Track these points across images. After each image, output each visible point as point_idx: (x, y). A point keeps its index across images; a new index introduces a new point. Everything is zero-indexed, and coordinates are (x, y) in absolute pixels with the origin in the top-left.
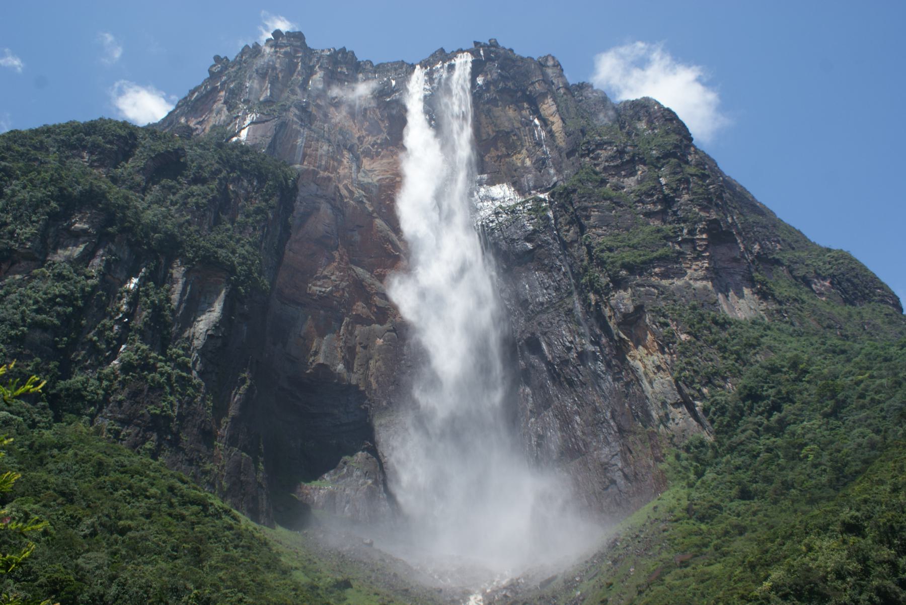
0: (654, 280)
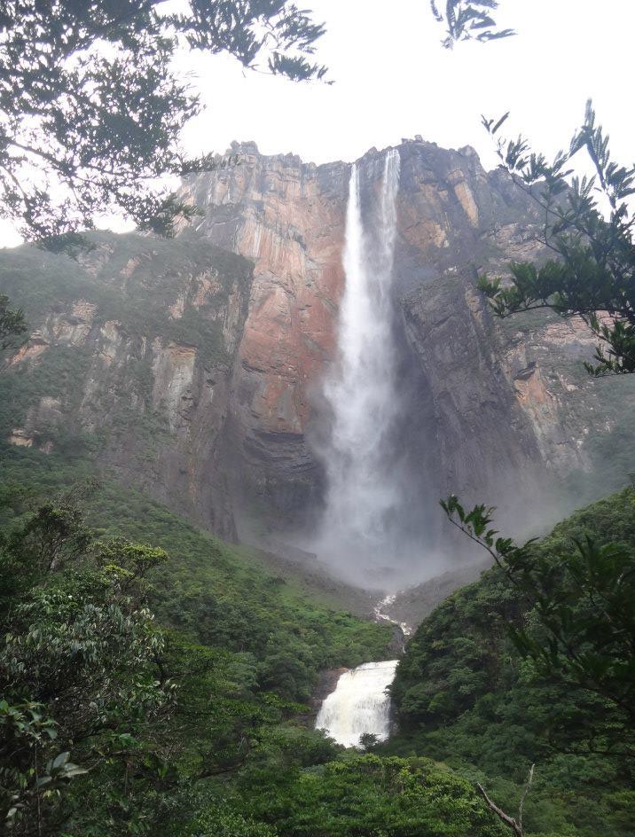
0: (547, 339)
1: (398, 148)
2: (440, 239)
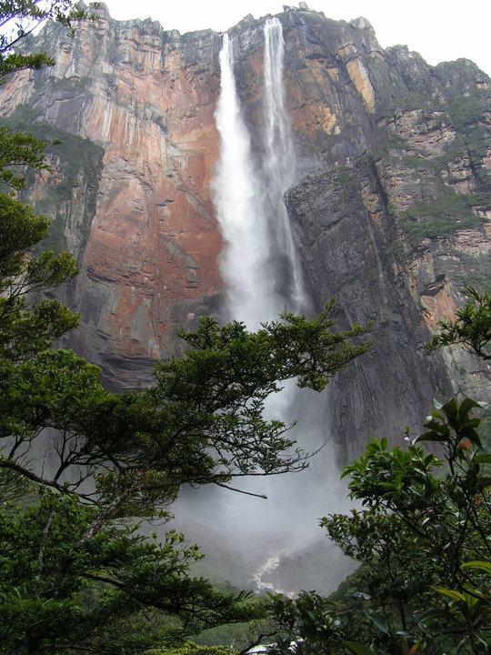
0: (458, 248)
1: (281, 17)
2: (330, 124)
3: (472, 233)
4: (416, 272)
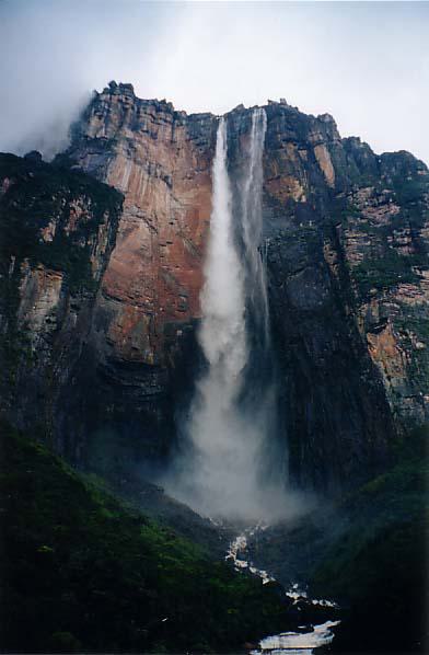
0: (398, 298)
3: (411, 286)
4: (364, 314)
